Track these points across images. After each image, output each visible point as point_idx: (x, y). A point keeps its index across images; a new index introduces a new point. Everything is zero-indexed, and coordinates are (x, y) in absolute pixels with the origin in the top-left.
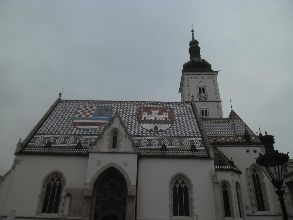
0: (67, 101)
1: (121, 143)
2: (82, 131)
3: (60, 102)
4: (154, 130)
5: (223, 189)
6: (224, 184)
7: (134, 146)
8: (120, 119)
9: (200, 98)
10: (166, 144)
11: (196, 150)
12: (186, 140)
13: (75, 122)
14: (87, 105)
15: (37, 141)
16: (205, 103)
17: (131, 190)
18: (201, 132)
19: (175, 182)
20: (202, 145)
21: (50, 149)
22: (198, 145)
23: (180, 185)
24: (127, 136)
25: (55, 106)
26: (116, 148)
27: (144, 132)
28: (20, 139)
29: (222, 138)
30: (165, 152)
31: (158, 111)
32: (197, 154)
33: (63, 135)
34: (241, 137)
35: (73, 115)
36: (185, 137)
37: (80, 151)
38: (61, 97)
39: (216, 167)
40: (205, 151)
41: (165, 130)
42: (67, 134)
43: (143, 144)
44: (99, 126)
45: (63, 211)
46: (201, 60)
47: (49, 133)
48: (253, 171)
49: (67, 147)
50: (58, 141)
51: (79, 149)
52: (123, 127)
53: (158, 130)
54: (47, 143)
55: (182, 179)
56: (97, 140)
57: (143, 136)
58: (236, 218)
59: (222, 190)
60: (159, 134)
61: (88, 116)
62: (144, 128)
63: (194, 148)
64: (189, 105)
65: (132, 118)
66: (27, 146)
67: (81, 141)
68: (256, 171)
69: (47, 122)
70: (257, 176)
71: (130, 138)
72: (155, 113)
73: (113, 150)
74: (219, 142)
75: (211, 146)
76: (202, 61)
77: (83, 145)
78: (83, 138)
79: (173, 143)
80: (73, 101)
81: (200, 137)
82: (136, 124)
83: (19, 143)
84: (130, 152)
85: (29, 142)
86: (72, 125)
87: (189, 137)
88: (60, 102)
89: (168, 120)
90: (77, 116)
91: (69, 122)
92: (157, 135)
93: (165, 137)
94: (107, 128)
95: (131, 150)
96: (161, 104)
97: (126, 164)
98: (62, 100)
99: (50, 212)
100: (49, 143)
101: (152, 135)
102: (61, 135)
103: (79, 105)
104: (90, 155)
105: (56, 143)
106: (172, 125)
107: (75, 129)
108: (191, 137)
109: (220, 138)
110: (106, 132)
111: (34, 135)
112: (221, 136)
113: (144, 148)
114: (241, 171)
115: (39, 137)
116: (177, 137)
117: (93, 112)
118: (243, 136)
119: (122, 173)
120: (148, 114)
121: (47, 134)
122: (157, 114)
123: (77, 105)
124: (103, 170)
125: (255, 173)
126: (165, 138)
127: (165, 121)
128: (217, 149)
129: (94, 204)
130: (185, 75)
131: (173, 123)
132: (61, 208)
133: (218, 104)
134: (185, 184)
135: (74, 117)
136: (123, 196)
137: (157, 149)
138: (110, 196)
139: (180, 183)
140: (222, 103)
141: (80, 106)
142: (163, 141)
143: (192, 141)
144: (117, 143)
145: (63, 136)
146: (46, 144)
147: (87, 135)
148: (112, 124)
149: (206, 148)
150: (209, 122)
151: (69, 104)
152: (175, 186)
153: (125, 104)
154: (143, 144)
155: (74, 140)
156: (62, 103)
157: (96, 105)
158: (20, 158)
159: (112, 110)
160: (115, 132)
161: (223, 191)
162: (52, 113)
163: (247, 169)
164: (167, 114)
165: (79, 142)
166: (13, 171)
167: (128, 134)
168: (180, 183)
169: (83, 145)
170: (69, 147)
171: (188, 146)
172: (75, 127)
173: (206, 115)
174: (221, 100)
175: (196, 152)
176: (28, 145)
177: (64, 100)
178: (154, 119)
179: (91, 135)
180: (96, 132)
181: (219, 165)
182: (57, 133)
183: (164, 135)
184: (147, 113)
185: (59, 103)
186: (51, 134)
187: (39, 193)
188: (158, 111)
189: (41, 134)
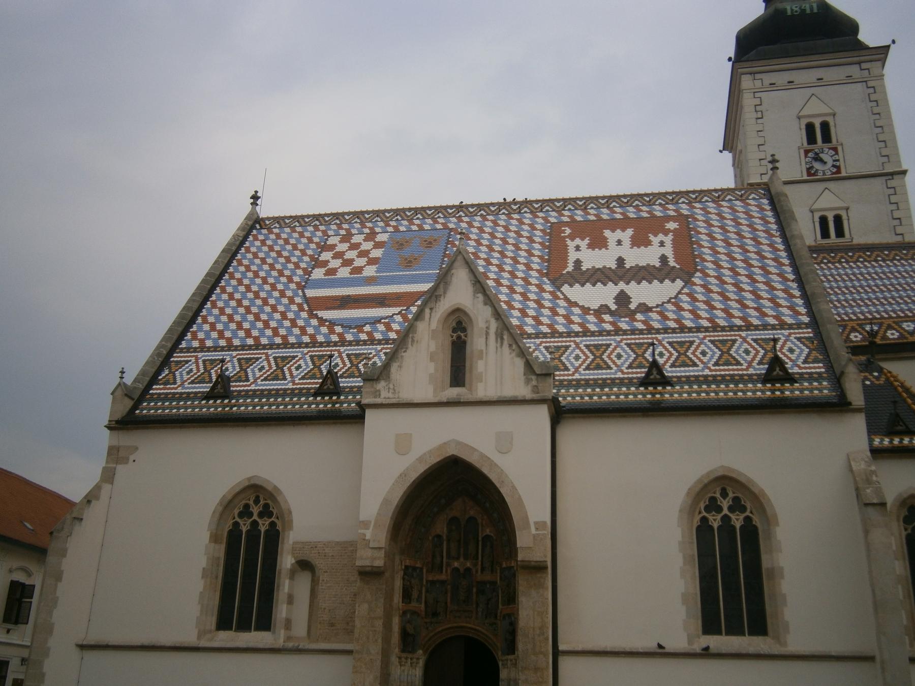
0: (279, 220)
1: (480, 366)
2: (338, 329)
4: (613, 307)
5: (906, 529)
7: (534, 372)
8: (472, 271)
9: (812, 167)
10: (661, 361)
11: (790, 378)
13: (310, 298)
14: (354, 231)
15: (182, 374)
16: (831, 185)
18: (808, 304)
19: (702, 505)
20: (814, 353)
21: (226, 401)
23: (726, 519)
24: (505, 337)
25: (238, 243)
26: (464, 386)
27: (576, 319)
28: (122, 372)
29: (905, 325)
30: (660, 393)
31: (630, 232)
32: (790, 391)
33: (271, 348)
35: (304, 270)
36: (740, 328)
37: (334, 404)
38: (258, 208)
39: (877, 442)
40: (824, 379)
41: (658, 306)
42: (286, 344)
43: (572, 364)
44: (399, 306)
45: (288, 624)
46: (811, 8)
47: (222, 343)
49: (285, 390)
50: (253, 372)
51: (331, 398)
52: (485, 304)
53: (633, 306)
54: (217, 382)
56: (392, 357)
57: (569, 334)
59: (904, 533)
60: (636, 320)
61: (359, 270)
62: (576, 304)
63: (778, 370)
64: (761, 198)
65: (528, 267)
66: (148, 396)
67: (337, 365)
69: (214, 305)
71: (517, 343)
72: (619, 242)
73: (454, 393)
74: (894, 339)
75: (853, 358)
76: (815, 10)
77: (343, 382)
78: (344, 355)
79: (693, 353)
80: (303, 217)
81: (807, 326)
82: (543, 290)
83: (119, 384)
84: (520, 398)
85: (154, 380)
86: (303, 310)
87: (756, 328)
89: (672, 263)
90: (318, 274)
91: (291, 300)
92: (624, 326)
93: (658, 331)
94: (427, 311)
95: (523, 391)
97: (505, 442)
98: (263, 220)
100: (223, 381)
101: (608, 327)
102: (264, 347)
103: (325, 233)
104: (369, 415)
105: (248, 380)
106: (688, 282)
107: (314, 322)
108: (765, 327)
109: (896, 323)
110: (421, 326)
111: (170, 354)
112: (899, 317)
113: (578, 381)
115: (187, 362)
116: (707, 329)
117: (377, 253)
119: (493, 477)
120: (591, 246)
121: (216, 348)
122: (627, 242)
123: (319, 234)
124: (422, 469)
126: (660, 337)
127: (659, 270)
128: (881, 370)
129: (397, 598)
130: (742, 76)
131: (692, 275)
132: (281, 611)
133: (892, 183)
134: (748, 513)
135: (308, 279)
136: (504, 565)
137: (630, 382)
138: (456, 564)
139: (726, 511)
140: (908, 178)
141: (329, 236)
142: (651, 348)
143: (772, 343)
144: (468, 364)
145: (270, 352)
146: (211, 385)
147: (358, 342)
148: (445, 293)
149: (830, 367)
150: (847, 262)
151: (287, 230)
152: (704, 520)
153: (497, 214)
154: (572, 364)
155: (310, 363)
156: (265, 231)
157: (388, 225)
158: (127, 439)
159: (448, 242)
160: (459, 323)
161: (908, 537)
162: (231, 270)
164: (668, 239)
165: (329, 372)
166: (106, 487)
167: (508, 330)
168: (726, 511)
169: (344, 383)
170: (293, 390)
171: (756, 362)
172: (312, 315)
173: (840, 233)
174: (904, 167)
175: (787, 385)
176: (151, 392)
177: (268, 219)
178: (614, 266)
179: (372, 341)
181: (891, 433)
182: (250, 341)
183: (656, 325)
184: (587, 241)
185: (255, 232)
186: (230, 347)
187: (202, 562)
188: (630, 232)
189: (195, 350)
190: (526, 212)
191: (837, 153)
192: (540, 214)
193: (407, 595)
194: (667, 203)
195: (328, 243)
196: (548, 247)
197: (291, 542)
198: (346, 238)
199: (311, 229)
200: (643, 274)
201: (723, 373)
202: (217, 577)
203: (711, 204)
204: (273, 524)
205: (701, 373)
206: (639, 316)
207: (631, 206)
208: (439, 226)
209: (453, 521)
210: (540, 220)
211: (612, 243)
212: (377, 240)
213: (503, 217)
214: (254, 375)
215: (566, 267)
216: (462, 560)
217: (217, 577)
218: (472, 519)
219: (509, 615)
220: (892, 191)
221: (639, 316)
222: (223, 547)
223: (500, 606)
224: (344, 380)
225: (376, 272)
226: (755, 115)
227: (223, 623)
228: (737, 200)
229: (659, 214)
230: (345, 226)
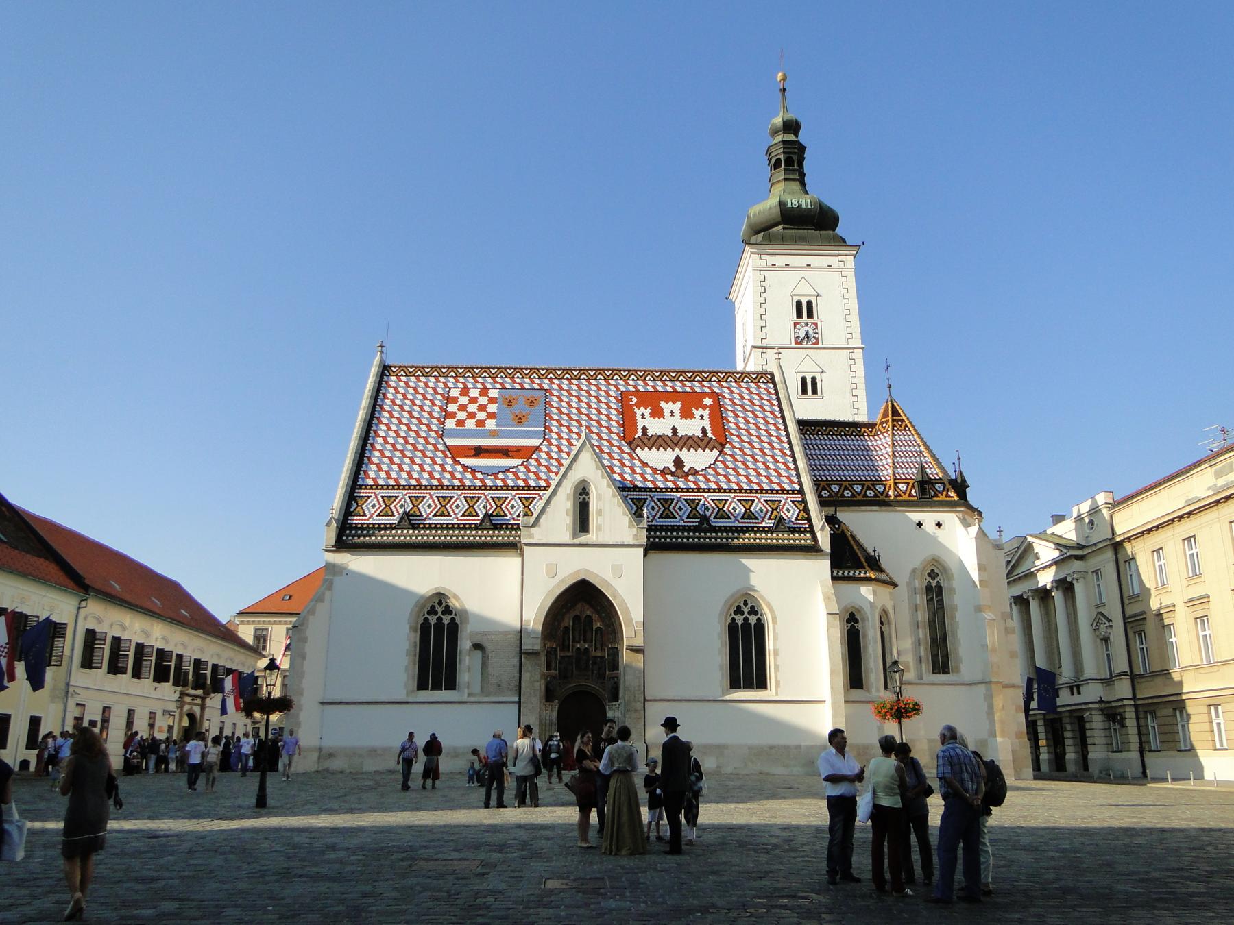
2: (479, 475)
3: (386, 372)
4: (673, 469)
6: (852, 615)
10: (708, 514)
12: (759, 501)
14: (470, 385)
15: (368, 507)
17: (631, 634)
22: (791, 513)
23: (746, 619)
29: (855, 487)
31: (679, 404)
34: (908, 484)
36: (756, 491)
40: (808, 532)
41: (703, 470)
42: (442, 487)
48: (929, 575)
49: (453, 524)
52: (603, 478)
53: (686, 469)
54: (402, 519)
55: (750, 605)
58: (873, 690)
62: (646, 465)
64: (768, 382)
68: (937, 575)
70: (939, 588)
72: (672, 413)
77: (495, 520)
82: (623, 452)
87: (767, 492)
88: (386, 372)
89: (710, 435)
90: (450, 424)
92: (682, 485)
96: (687, 380)
97: (619, 571)
98: (390, 367)
99: (436, 687)
108: (772, 491)
112: (852, 480)
113: (656, 526)
114: (895, 580)
117: (492, 408)
118: (912, 482)
120: (653, 415)
121: (388, 487)
125: (933, 579)
126: (706, 495)
127: (702, 440)
128: (839, 523)
129: (544, 667)
131: (723, 446)
132: (463, 676)
137: (688, 529)
138: (578, 646)
141: (450, 389)
145: (432, 492)
147: (497, 488)
150: (822, 435)
151: (413, 379)
152: (733, 619)
159: (546, 403)
163: (914, 571)
164: (706, 413)
168: (746, 614)
178: (670, 435)
179: (506, 487)
180: (518, 478)
184: (649, 410)
186: (398, 486)
188: (679, 404)
190: (600, 379)
191: (817, 328)
192: (612, 382)
193: (548, 667)
194: (703, 381)
195: (451, 395)
196: (622, 413)
197: (468, 632)
198: (465, 391)
199: (432, 379)
200: (690, 442)
201: (747, 525)
202: (415, 655)
203: (734, 384)
204: (453, 620)
205: (733, 525)
206: (691, 478)
207: (677, 380)
208: (537, 387)
209: (577, 618)
210: (612, 388)
211: (667, 413)
212: (490, 395)
213: (584, 382)
214: (425, 511)
215: (637, 432)
216: (582, 642)
217: (415, 655)
218: (589, 617)
219: (613, 678)
220: (853, 362)
221: (691, 478)
222: (418, 633)
223: (607, 672)
224: (494, 518)
225: (497, 425)
226: (760, 289)
227: (422, 685)
228: (752, 382)
229: (698, 390)
230: (461, 379)
